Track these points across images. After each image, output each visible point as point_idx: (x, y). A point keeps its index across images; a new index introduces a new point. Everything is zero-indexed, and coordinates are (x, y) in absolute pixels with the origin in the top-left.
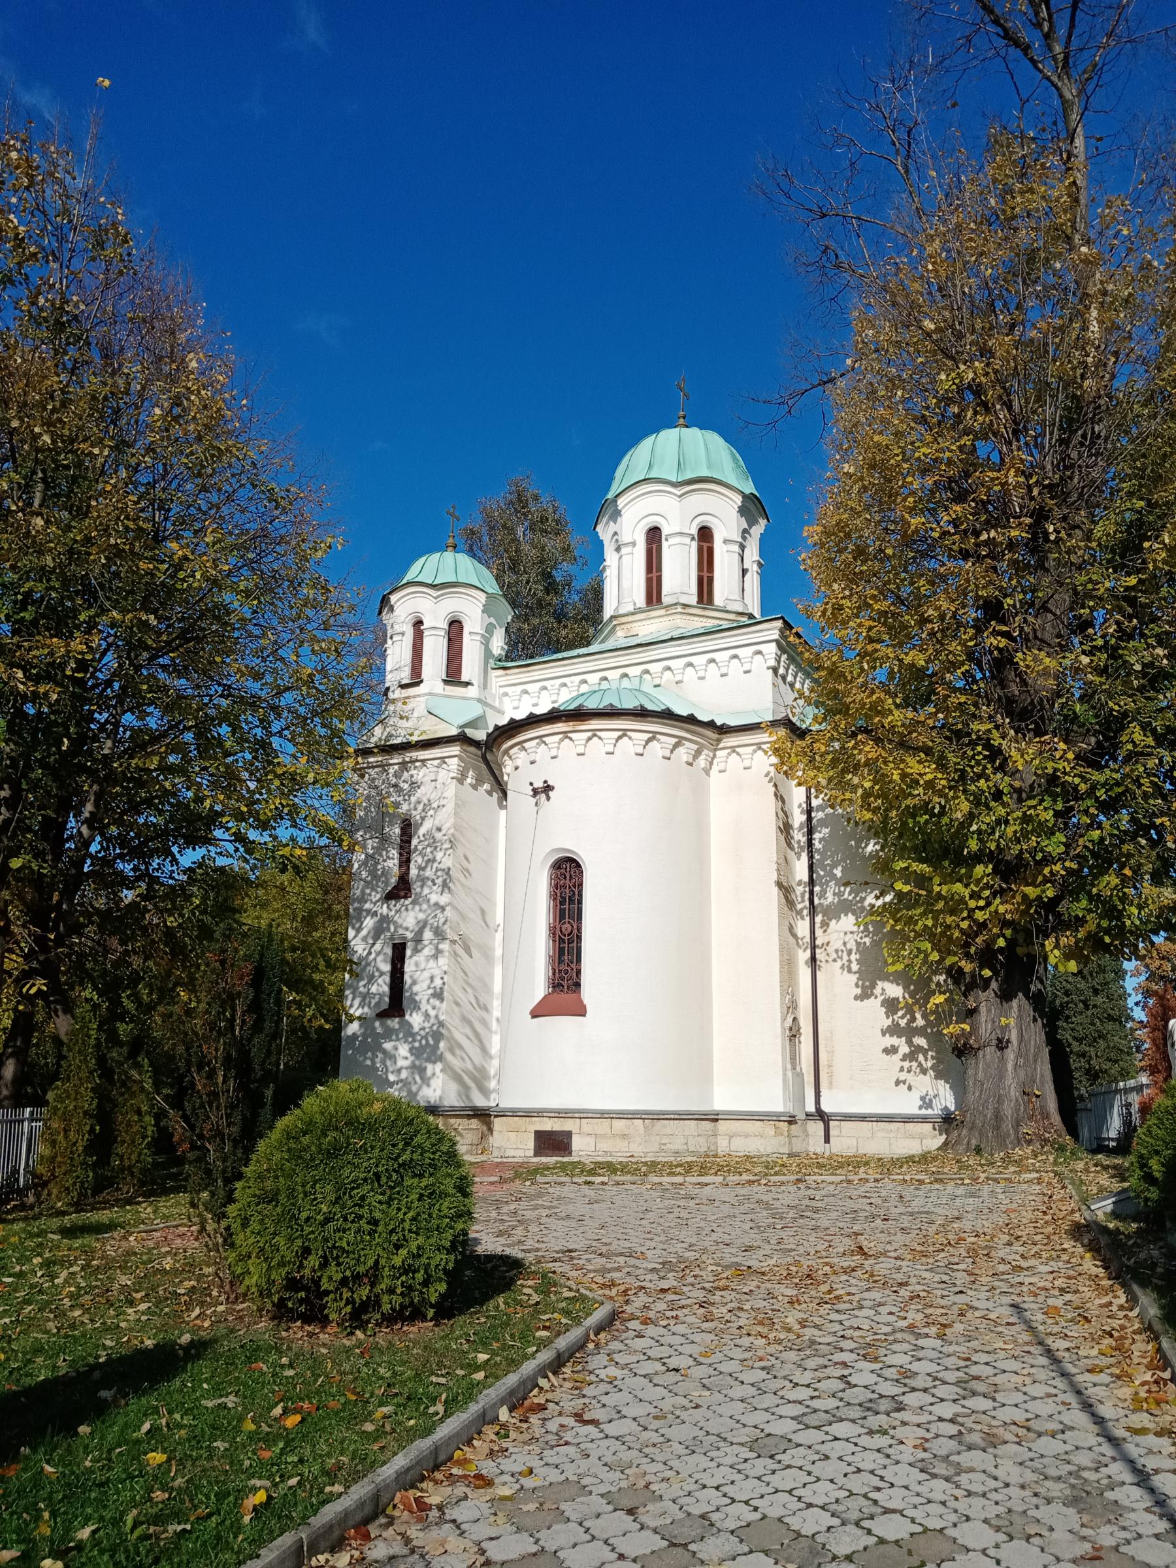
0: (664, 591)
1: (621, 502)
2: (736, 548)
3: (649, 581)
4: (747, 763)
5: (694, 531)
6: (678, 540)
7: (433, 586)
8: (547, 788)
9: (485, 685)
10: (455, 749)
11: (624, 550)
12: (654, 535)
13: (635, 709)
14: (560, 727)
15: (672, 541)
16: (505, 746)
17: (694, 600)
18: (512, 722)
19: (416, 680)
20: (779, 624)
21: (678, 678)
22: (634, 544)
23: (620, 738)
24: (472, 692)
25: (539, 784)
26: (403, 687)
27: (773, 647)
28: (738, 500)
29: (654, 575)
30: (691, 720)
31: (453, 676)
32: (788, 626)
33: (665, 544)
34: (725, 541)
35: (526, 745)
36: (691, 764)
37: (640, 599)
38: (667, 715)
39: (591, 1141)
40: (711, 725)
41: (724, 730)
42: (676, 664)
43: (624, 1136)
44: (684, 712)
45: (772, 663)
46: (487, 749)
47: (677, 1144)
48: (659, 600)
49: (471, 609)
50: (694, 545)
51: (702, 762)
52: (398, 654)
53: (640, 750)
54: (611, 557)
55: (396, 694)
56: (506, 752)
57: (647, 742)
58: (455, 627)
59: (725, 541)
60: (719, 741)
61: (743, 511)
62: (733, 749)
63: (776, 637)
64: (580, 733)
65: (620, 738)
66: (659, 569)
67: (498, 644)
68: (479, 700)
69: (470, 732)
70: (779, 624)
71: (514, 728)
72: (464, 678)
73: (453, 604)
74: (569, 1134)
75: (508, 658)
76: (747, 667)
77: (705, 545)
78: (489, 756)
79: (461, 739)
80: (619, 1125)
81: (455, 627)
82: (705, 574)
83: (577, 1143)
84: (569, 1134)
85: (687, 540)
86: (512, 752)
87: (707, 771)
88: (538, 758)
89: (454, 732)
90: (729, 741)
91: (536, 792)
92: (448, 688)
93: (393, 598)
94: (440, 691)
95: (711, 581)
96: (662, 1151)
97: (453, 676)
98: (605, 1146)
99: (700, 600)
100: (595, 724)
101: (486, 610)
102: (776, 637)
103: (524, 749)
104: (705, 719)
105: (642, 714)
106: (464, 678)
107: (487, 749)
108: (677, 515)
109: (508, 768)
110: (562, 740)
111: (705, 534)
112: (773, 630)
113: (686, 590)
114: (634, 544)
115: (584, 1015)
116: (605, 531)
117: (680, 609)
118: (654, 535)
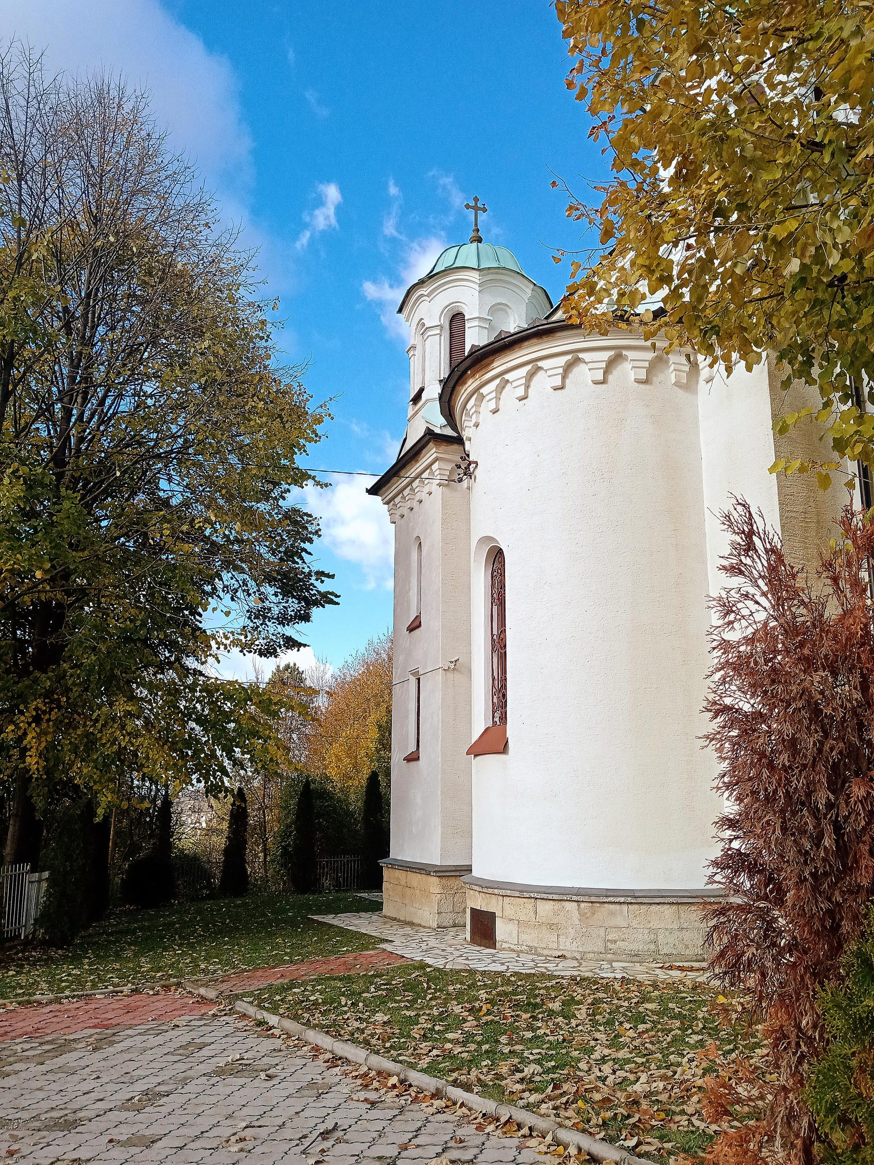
14: (471, 385)
23: (530, 376)
36: (646, 382)
39: (512, 927)
43: (551, 926)
47: (638, 942)
57: (568, 368)
65: (530, 376)
74: (492, 916)
80: (545, 908)
83: (502, 930)
84: (492, 916)
96: (607, 951)
98: (529, 938)
100: (500, 364)
115: (504, 750)
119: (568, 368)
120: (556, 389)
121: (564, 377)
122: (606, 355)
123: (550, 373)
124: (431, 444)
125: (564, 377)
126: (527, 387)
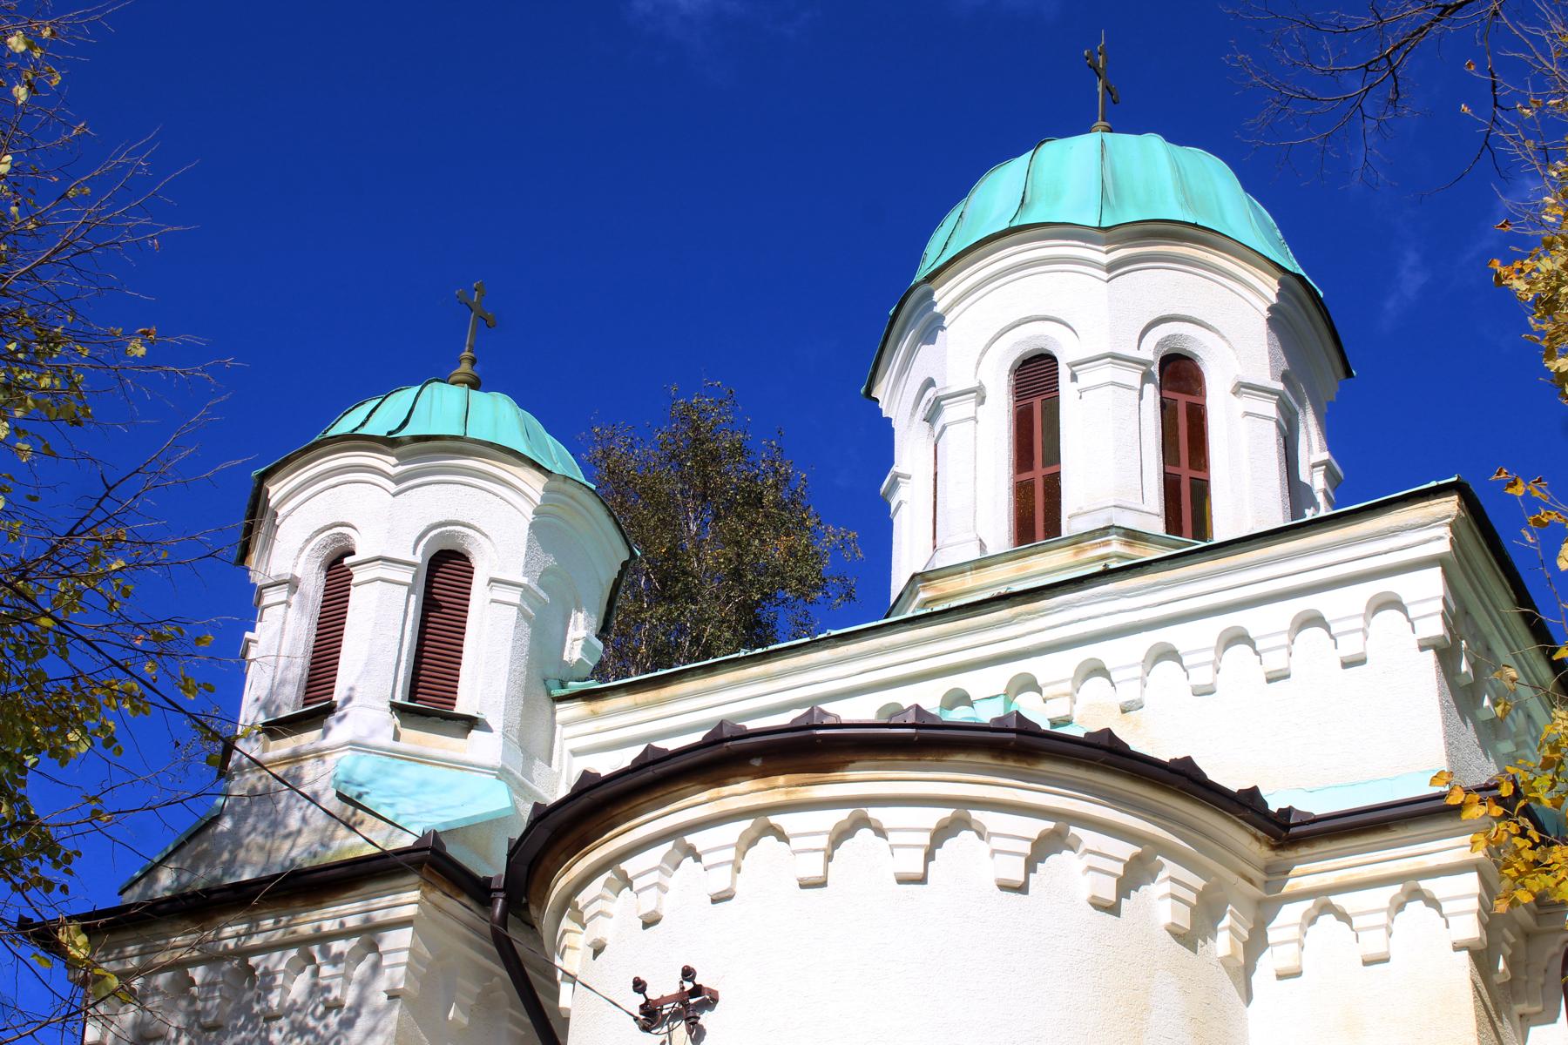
0: (1068, 505)
1: (943, 296)
2: (1270, 408)
3: (1023, 492)
4: (1374, 944)
5: (1149, 352)
6: (1107, 372)
7: (388, 443)
8: (694, 1001)
9: (532, 744)
10: (407, 901)
11: (950, 413)
12: (1036, 377)
13: (998, 726)
14: (744, 793)
15: (1087, 377)
16: (562, 883)
17: (1157, 526)
18: (588, 784)
19: (316, 708)
20: (1449, 506)
21: (1128, 693)
22: (979, 394)
23: (941, 834)
24: (480, 747)
25: (664, 985)
26: (277, 728)
27: (1432, 583)
28: (1269, 288)
29: (1039, 473)
30: (1183, 779)
31: (429, 697)
32: (1480, 522)
33: (1067, 390)
34: (1242, 388)
35: (630, 866)
37: (998, 529)
38: (1104, 755)
40: (1245, 805)
41: (1288, 833)
42: (1122, 654)
44: (1165, 753)
45: (1435, 628)
46: (510, 891)
48: (1053, 527)
49: (503, 517)
50: (1151, 391)
51: (1223, 943)
52: (276, 645)
53: (1017, 874)
54: (910, 452)
55: (250, 748)
56: (568, 901)
58: (445, 574)
59: (1242, 388)
60: (1275, 874)
61: (1278, 319)
62: (1323, 901)
63: (1444, 547)
64: (810, 810)
65: (941, 834)
66: (1053, 455)
67: (579, 638)
68: (502, 773)
69: (453, 850)
70: (1449, 506)
71: (595, 808)
72: (461, 707)
73: (441, 502)
75: (600, 671)
76: (1350, 647)
77: (1182, 400)
78: (515, 934)
79: (431, 861)
81: (445, 574)
82: (1185, 473)
85: (1133, 377)
86: (582, 899)
87: (1243, 974)
88: (667, 907)
89: (408, 841)
90: (1312, 871)
91: (650, 1016)
92: (408, 734)
93: (276, 491)
94: (385, 740)
95: (1201, 491)
97: (429, 697)
99: (1173, 522)
100: (859, 781)
101: (543, 529)
102: (1444, 547)
103: (627, 882)
104: (1234, 783)
105: (1018, 745)
106: (461, 707)
107: (510, 891)
108: (1097, 316)
109: (572, 957)
110: (750, 841)
111: (1178, 375)
112: (1429, 527)
113: (1134, 501)
114: (979, 394)
116: (895, 397)
117: (1116, 546)
118: (1036, 377)
119: (1042, 849)
120: (1005, 887)
121: (1030, 867)
122: (1127, 850)
123: (997, 843)
124: (415, 878)
125: (1030, 867)
126: (929, 856)
